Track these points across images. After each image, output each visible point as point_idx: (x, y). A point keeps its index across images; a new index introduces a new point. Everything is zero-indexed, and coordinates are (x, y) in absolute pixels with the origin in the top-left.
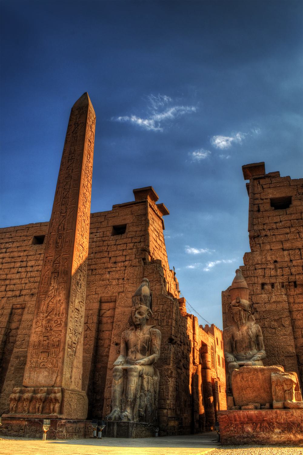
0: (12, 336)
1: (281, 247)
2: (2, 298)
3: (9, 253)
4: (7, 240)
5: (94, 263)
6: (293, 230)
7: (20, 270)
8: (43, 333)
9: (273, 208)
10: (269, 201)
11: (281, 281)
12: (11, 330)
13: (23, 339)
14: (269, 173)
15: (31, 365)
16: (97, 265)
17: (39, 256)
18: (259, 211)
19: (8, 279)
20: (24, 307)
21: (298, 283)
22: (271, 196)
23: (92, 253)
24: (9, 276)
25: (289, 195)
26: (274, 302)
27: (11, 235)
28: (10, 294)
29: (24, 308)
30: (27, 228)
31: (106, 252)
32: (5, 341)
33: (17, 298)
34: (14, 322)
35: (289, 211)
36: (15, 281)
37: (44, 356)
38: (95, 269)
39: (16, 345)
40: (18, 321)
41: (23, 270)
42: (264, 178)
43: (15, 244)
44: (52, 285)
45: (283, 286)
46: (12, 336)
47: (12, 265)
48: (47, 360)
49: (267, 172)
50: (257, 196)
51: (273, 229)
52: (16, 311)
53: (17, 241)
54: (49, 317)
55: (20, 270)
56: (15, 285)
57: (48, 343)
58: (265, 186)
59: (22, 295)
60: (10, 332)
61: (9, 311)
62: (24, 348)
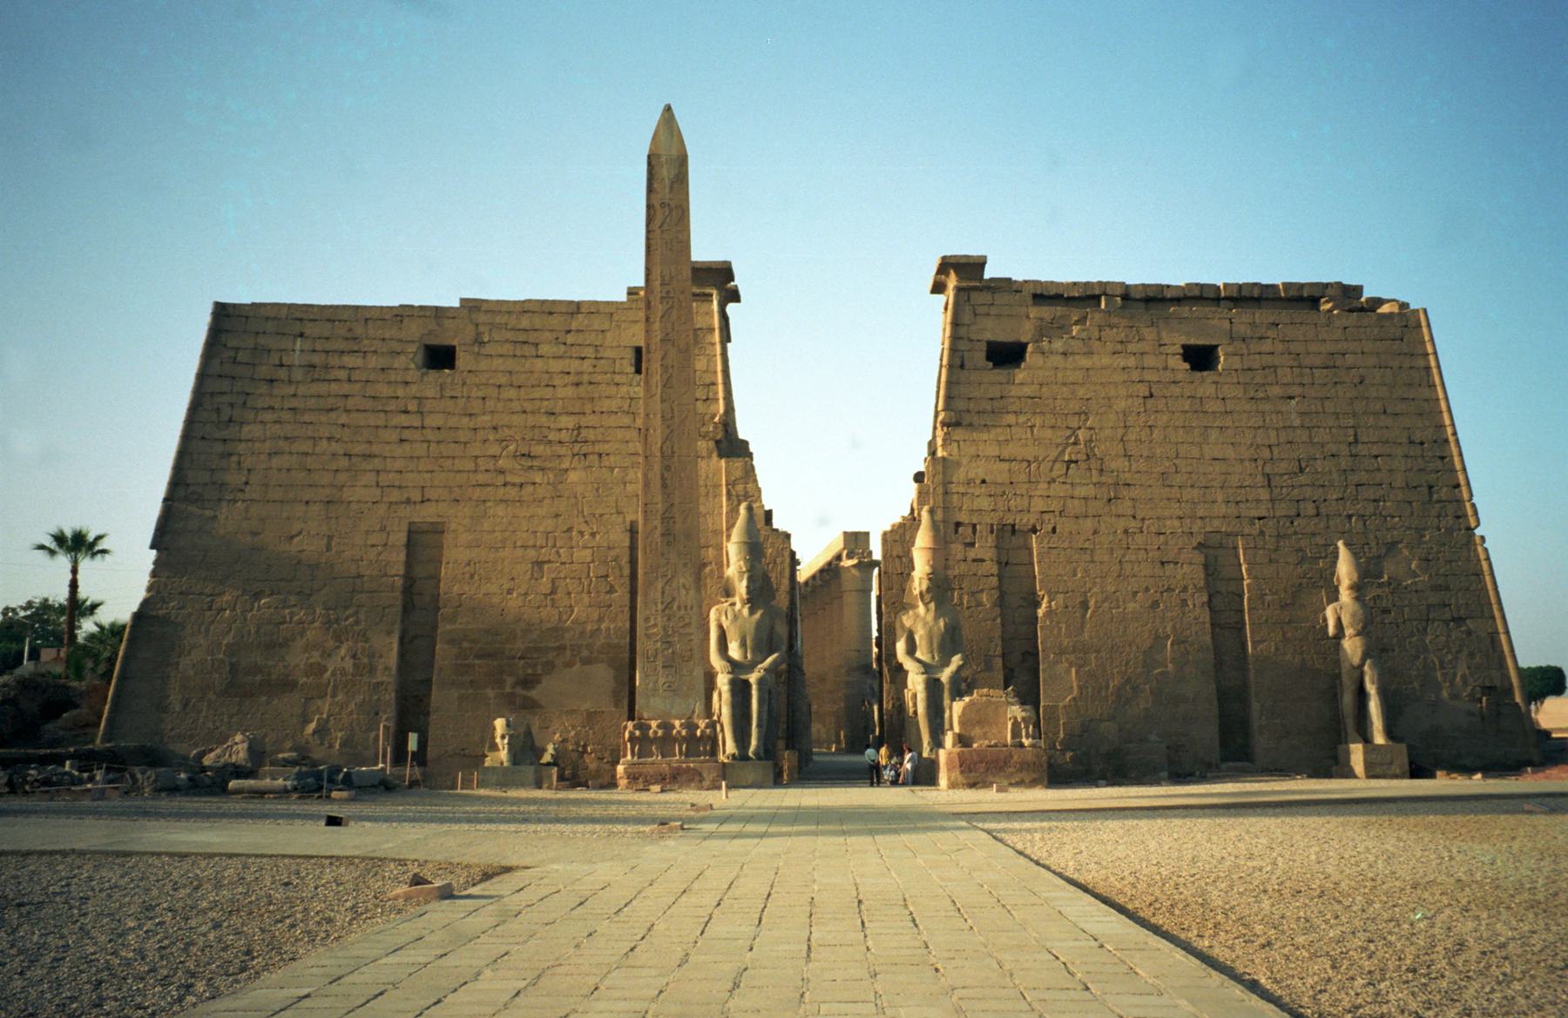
1: (997, 453)
2: (374, 503)
3: (359, 385)
4: (342, 345)
5: (600, 438)
6: (1022, 419)
7: (406, 434)
9: (991, 364)
10: (984, 347)
11: (990, 521)
14: (992, 280)
16: (610, 444)
17: (450, 403)
18: (962, 366)
19: (375, 456)
21: (1017, 527)
22: (989, 336)
24: (375, 449)
25: (1024, 340)
26: (974, 561)
27: (350, 330)
28: (395, 496)
30: (397, 315)
31: (628, 413)
33: (418, 506)
35: (1020, 375)
36: (399, 464)
38: (607, 454)
41: (416, 435)
42: (980, 289)
43: (373, 362)
45: (992, 532)
47: (380, 420)
49: (987, 275)
50: (963, 331)
51: (984, 412)
53: (375, 352)
54: (667, 612)
55: (406, 434)
56: (401, 472)
57: (673, 653)
58: (981, 310)
59: (429, 500)
60: (411, 586)
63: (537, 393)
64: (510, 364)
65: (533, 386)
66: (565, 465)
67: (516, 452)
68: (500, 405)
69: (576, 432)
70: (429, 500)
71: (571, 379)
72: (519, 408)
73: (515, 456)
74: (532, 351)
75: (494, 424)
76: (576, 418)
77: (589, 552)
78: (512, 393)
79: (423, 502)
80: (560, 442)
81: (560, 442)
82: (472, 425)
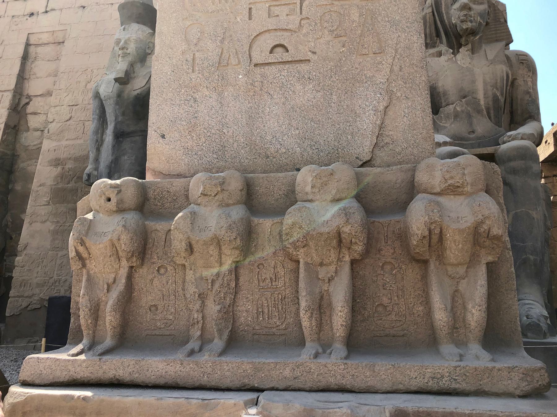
0: (35, 114)
12: (29, 97)
13: (68, 118)
20: (61, 41)
29: (63, 42)
32: (15, 126)
33: (41, 17)
34: (37, 78)
39: (48, 132)
40: (49, 75)
46: (35, 114)
48: (295, 19)
52: (39, 50)
59: (53, 10)
60: (28, 104)
61: (20, 50)
62: (75, 139)
70: (53, 10)
79: (46, 12)
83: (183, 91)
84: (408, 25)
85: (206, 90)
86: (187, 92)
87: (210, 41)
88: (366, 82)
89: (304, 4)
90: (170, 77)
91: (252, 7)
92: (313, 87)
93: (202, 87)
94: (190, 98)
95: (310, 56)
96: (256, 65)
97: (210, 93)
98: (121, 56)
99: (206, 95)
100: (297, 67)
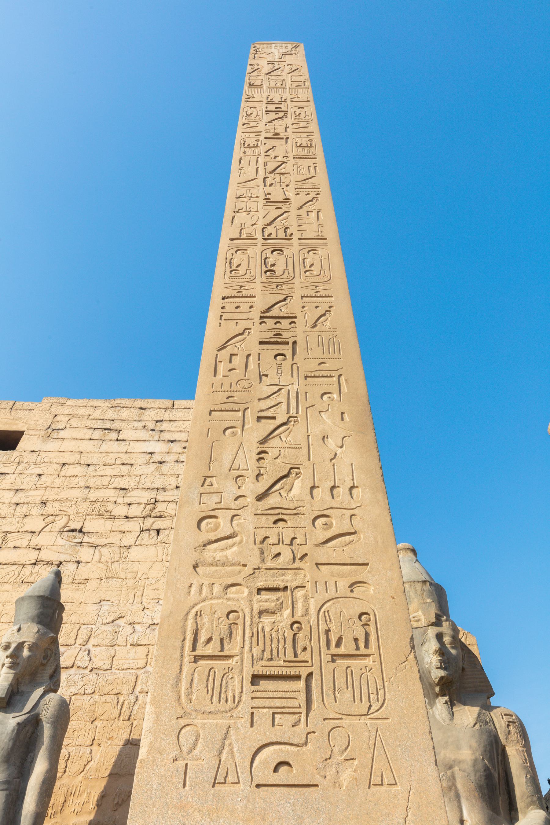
8: (248, 570)
15: (181, 764)
23: (177, 487)
37: (278, 703)
44: (273, 378)
63: (109, 471)
64: (86, 446)
65: (105, 465)
66: (125, 543)
67: (64, 527)
68: (59, 482)
69: (150, 507)
71: (157, 458)
72: (82, 484)
73: (61, 532)
74: (114, 435)
75: (44, 499)
76: (154, 493)
77: (142, 651)
78: (78, 470)
80: (127, 517)
81: (127, 517)
82: (15, 500)
83: (170, 812)
84: (420, 752)
85: (197, 814)
86: (174, 814)
87: (207, 749)
88: (382, 821)
89: (310, 715)
90: (156, 791)
91: (255, 712)
92: (323, 822)
93: (193, 810)
94: (178, 823)
95: (318, 780)
96: (258, 786)
97: (203, 819)
98: (6, 665)
99: (197, 821)
100: (305, 793)
